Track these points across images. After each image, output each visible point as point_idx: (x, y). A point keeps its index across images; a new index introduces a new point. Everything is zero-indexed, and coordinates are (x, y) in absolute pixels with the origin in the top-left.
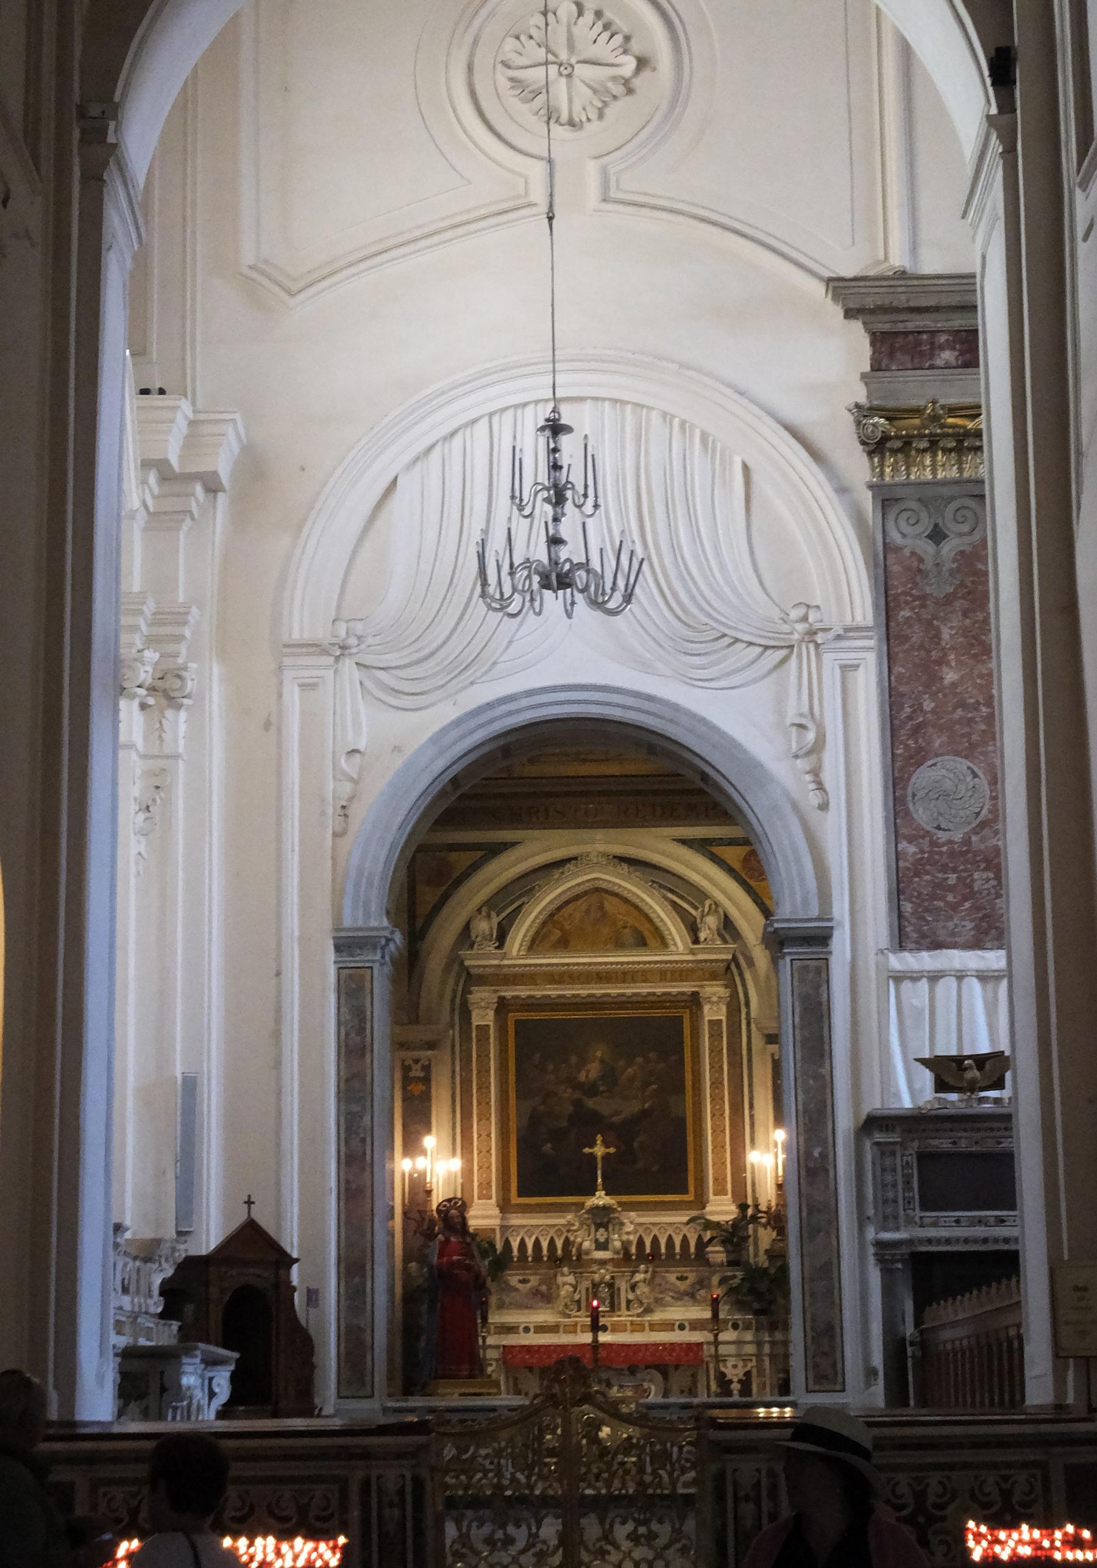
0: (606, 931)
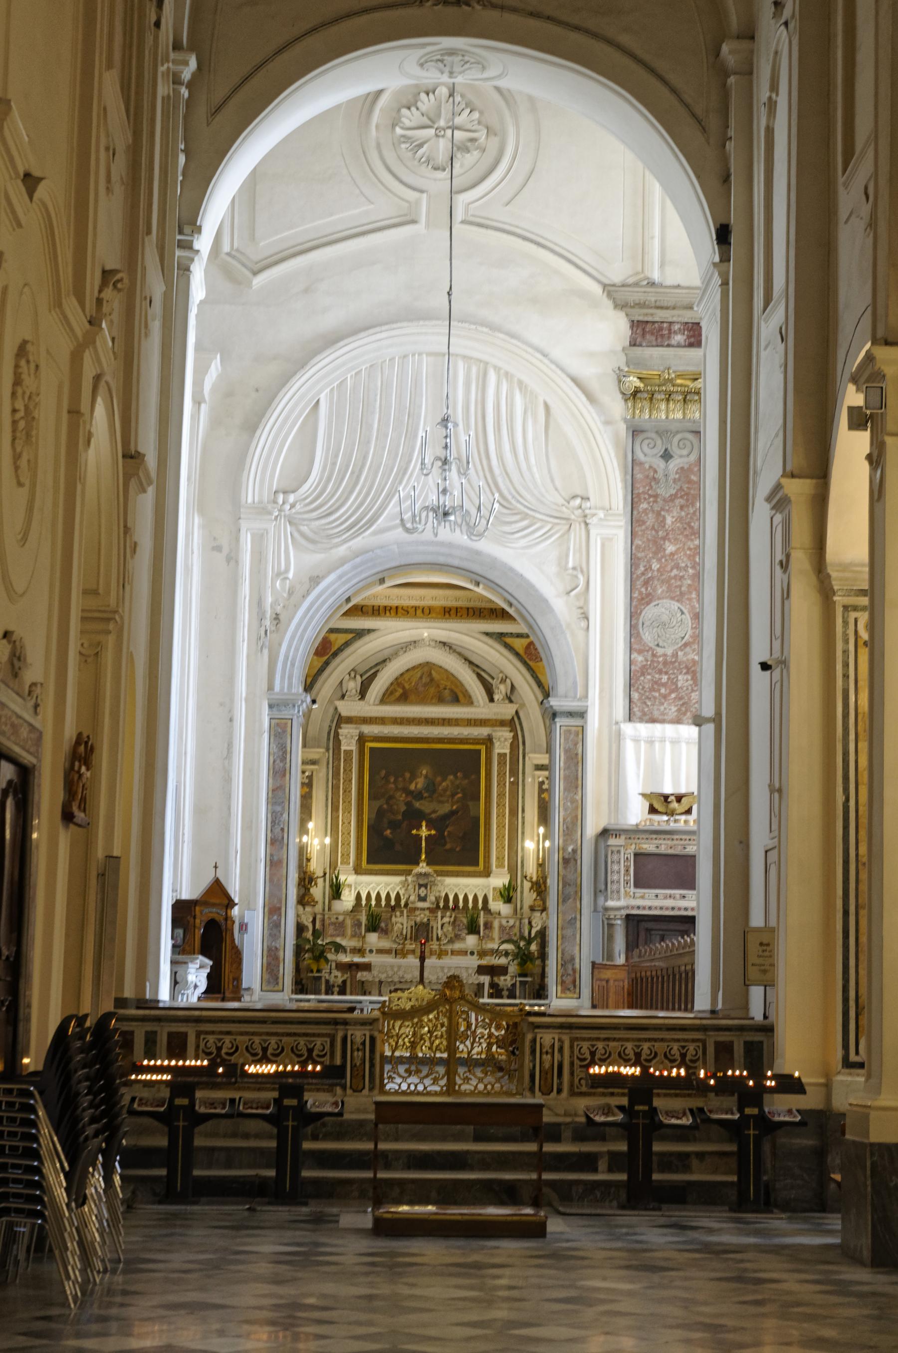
0: (432, 690)
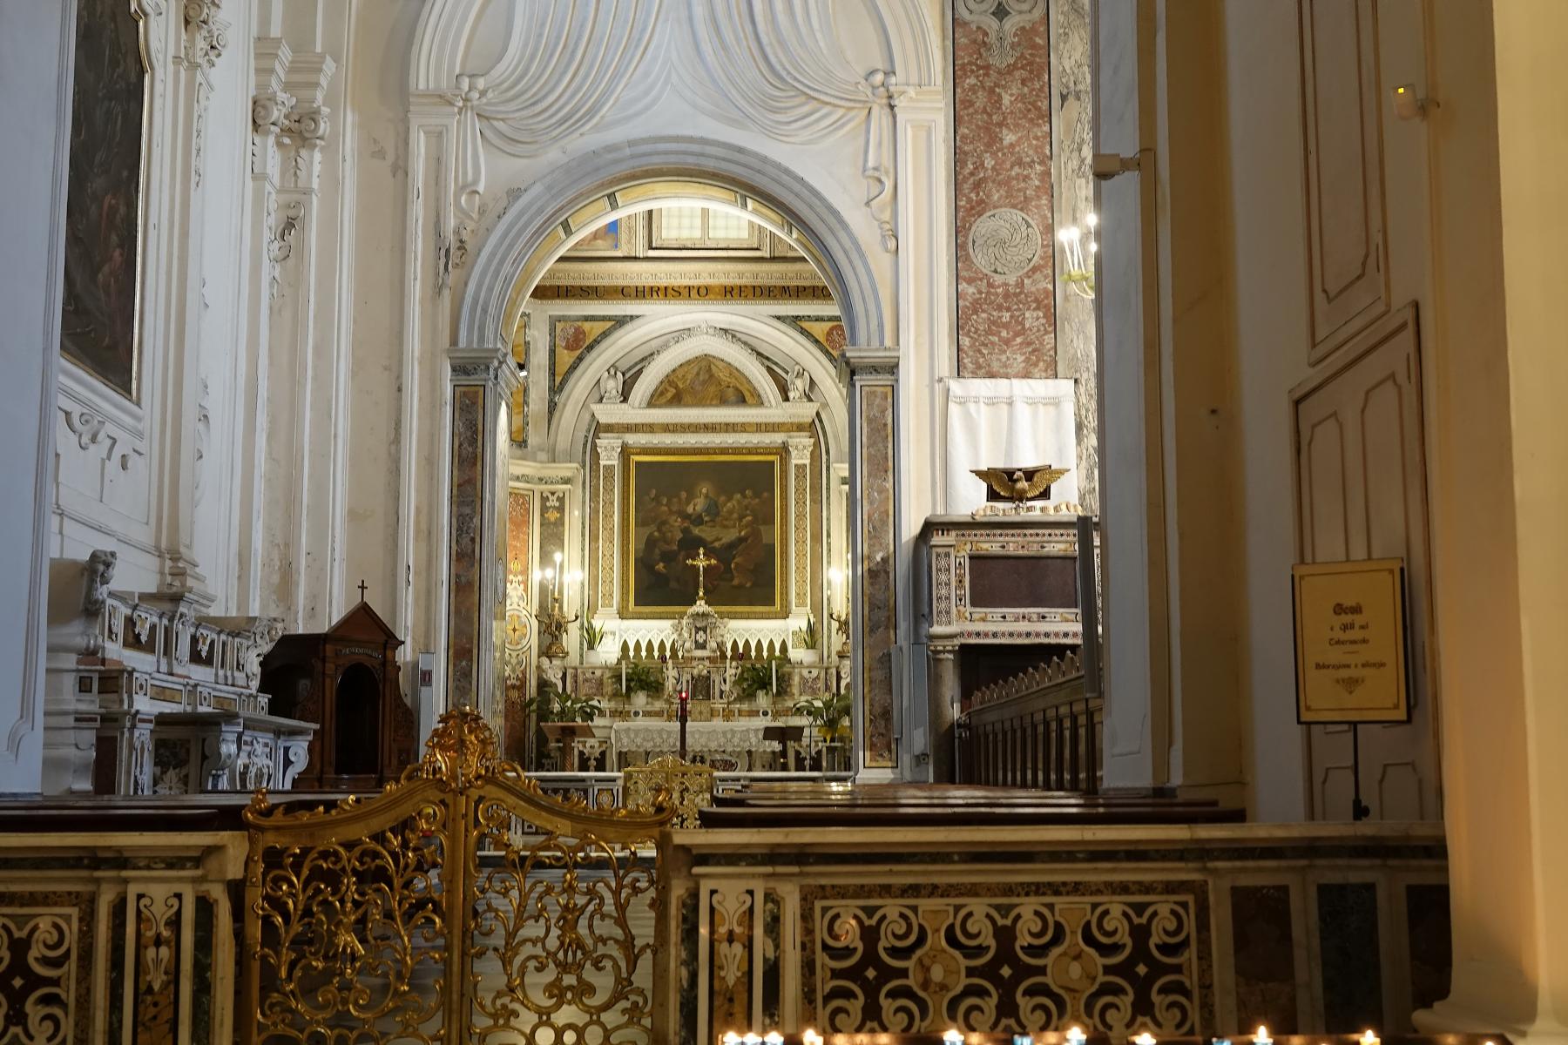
0: (712, 389)
